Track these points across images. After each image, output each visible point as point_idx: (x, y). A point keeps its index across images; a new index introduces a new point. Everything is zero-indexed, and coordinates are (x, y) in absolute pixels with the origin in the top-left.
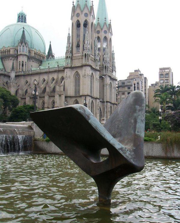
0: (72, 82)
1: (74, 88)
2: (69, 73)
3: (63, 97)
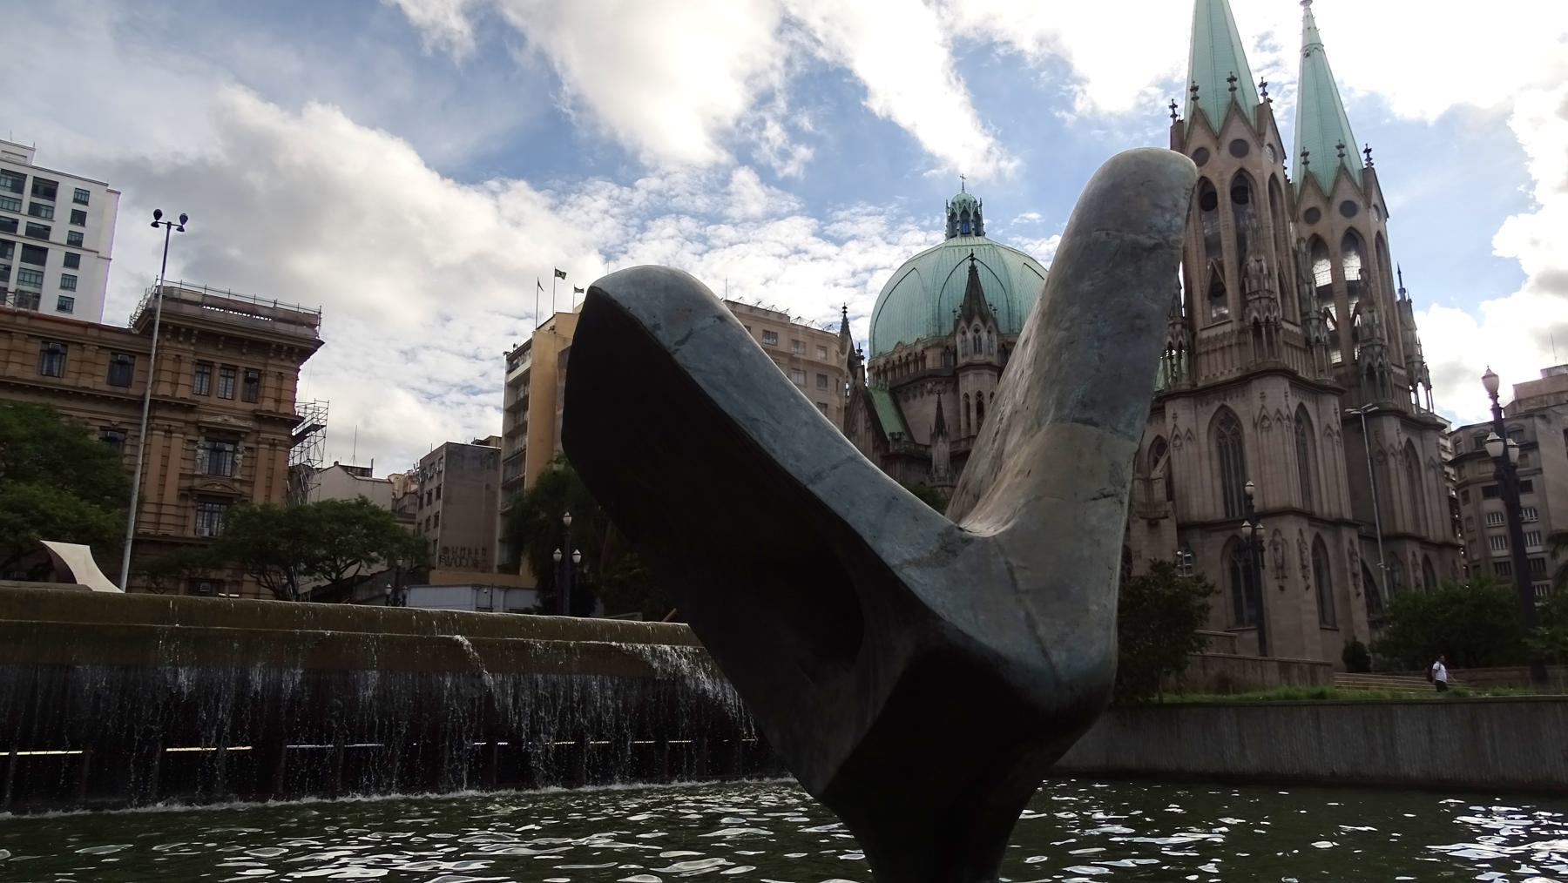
2: (1182, 418)
3: (1169, 530)
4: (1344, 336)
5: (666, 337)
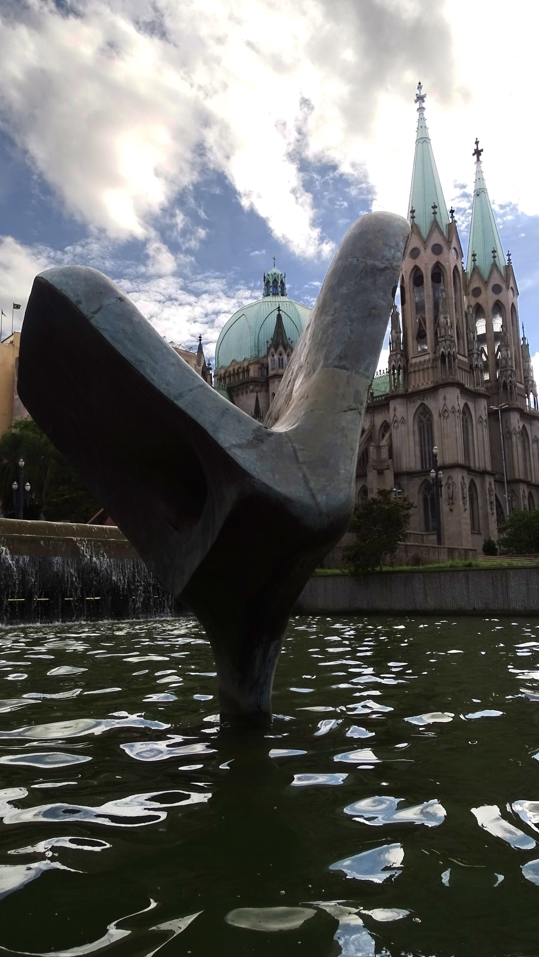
0: (411, 433)
1: (418, 449)
2: (399, 410)
3: (389, 476)
4: (491, 364)
5: (85, 309)
